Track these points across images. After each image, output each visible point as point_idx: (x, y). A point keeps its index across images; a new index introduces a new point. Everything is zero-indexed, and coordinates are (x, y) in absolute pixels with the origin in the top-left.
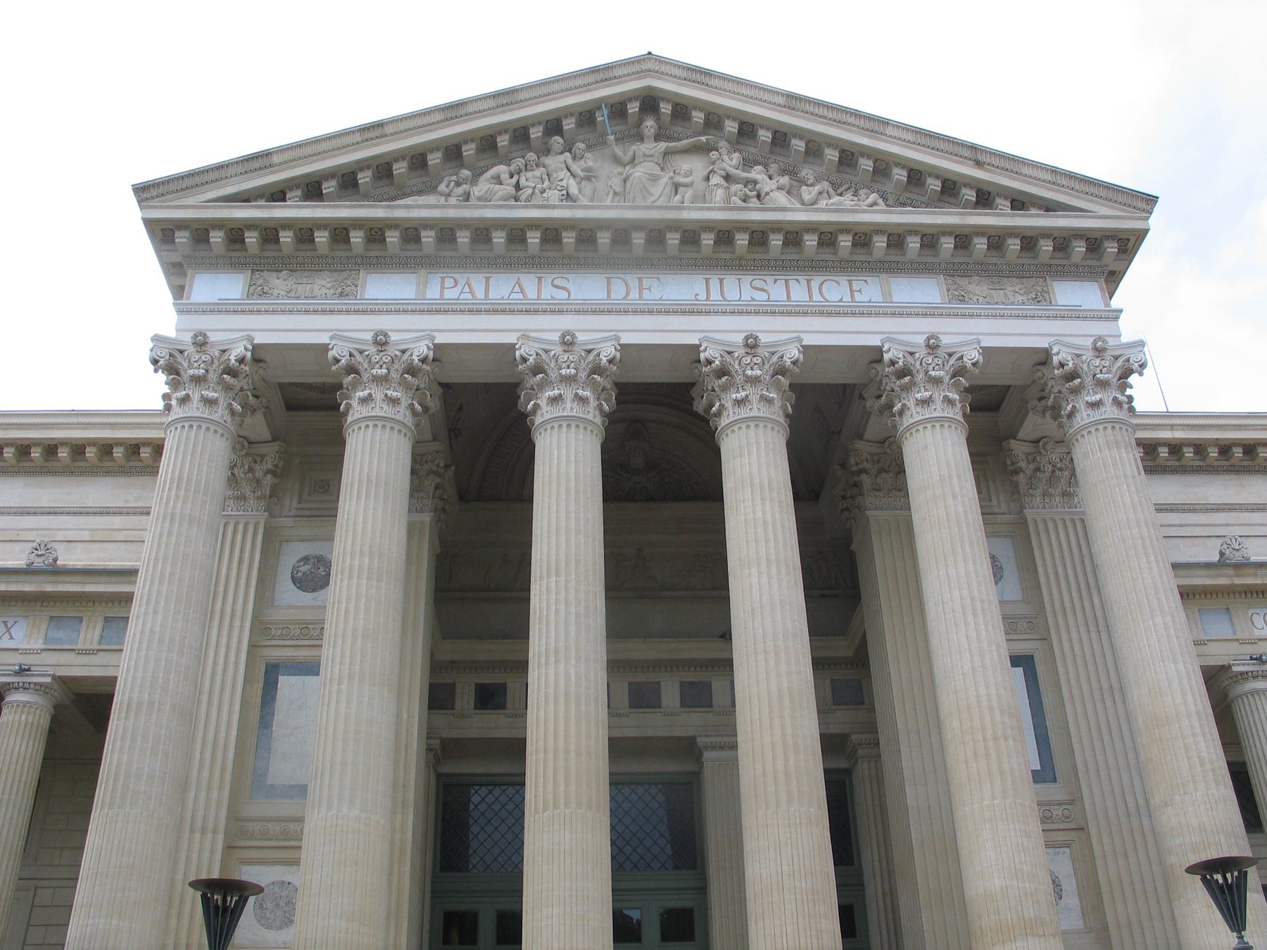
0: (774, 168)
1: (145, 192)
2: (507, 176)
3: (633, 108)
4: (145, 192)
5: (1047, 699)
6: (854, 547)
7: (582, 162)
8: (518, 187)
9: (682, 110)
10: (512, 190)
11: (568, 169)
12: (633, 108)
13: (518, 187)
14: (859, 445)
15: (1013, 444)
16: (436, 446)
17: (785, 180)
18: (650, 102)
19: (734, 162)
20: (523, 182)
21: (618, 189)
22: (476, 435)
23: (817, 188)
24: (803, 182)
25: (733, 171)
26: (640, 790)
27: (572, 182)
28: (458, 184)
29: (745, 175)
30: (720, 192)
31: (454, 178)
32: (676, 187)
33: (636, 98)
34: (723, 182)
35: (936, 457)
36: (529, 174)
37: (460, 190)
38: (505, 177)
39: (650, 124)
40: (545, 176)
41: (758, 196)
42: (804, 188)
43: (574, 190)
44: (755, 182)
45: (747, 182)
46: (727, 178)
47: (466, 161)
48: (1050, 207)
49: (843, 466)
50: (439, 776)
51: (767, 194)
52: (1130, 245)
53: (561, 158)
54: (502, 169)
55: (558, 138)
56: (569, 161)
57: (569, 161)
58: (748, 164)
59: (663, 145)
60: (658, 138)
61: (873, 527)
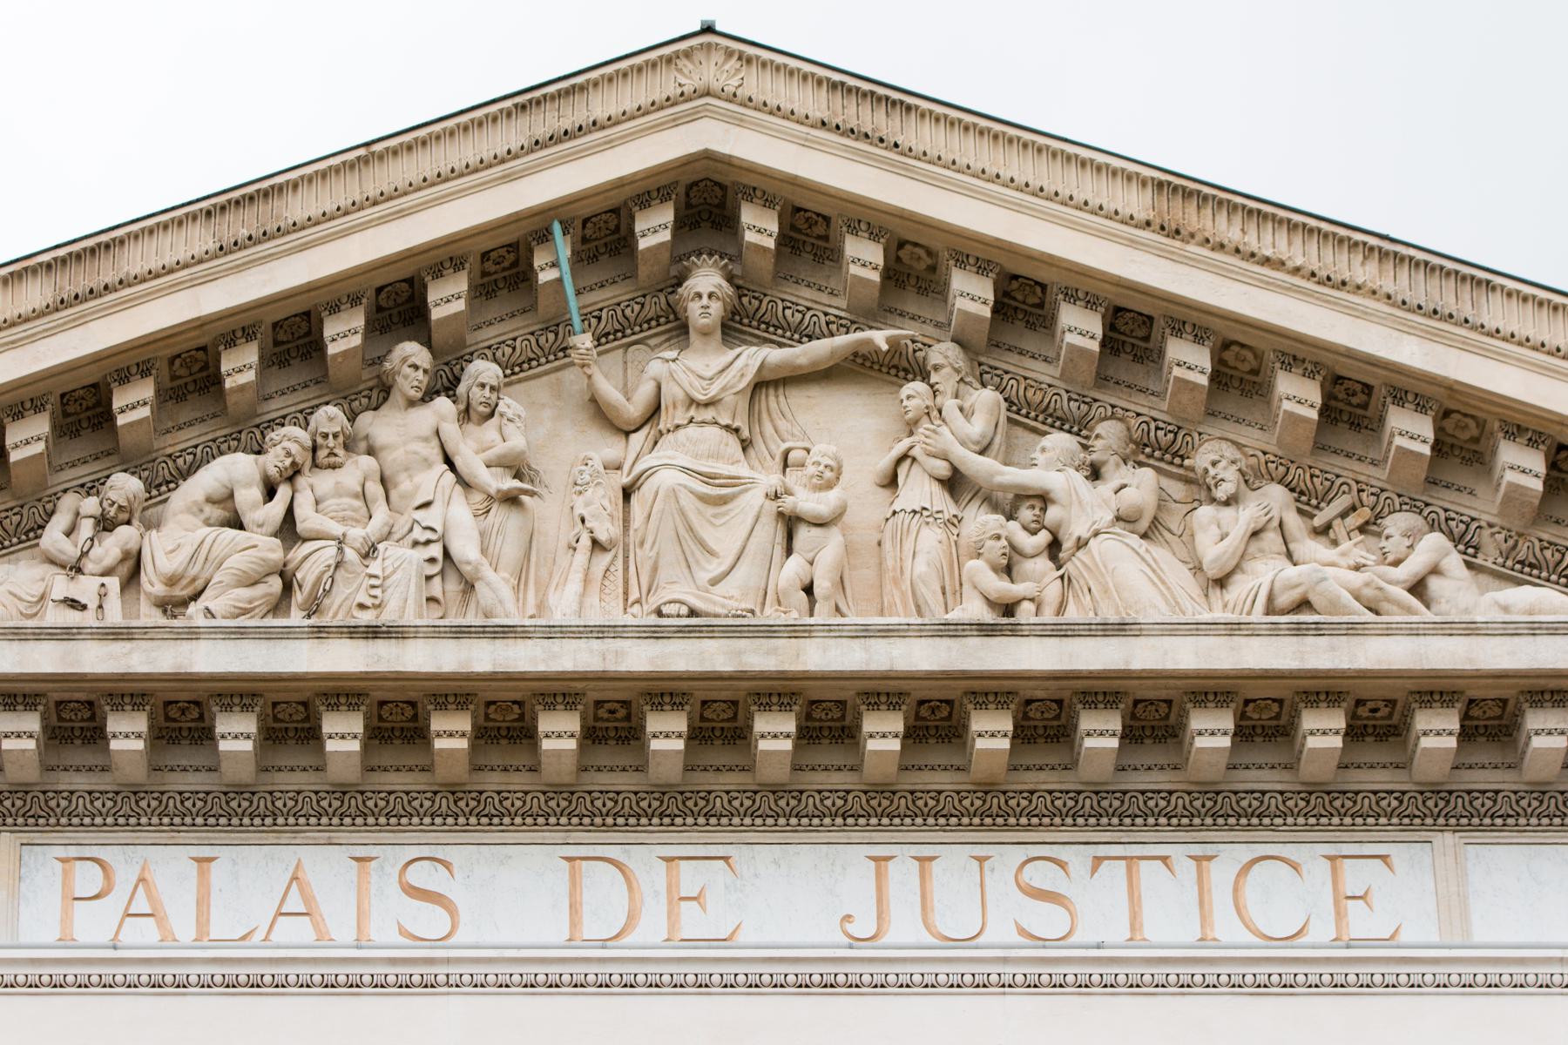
0: (1109, 434)
2: (256, 493)
7: (489, 431)
9: (812, 227)
11: (448, 461)
13: (288, 529)
19: (978, 427)
24: (1202, 488)
28: (106, 524)
31: (91, 505)
32: (790, 523)
34: (940, 500)
36: (324, 482)
37: (111, 547)
38: (249, 497)
40: (375, 489)
41: (1054, 547)
42: (1205, 512)
43: (466, 549)
44: (1044, 499)
45: (1011, 503)
46: (954, 483)
51: (1081, 544)
54: (236, 469)
56: (451, 430)
57: (451, 430)
60: (734, 328)
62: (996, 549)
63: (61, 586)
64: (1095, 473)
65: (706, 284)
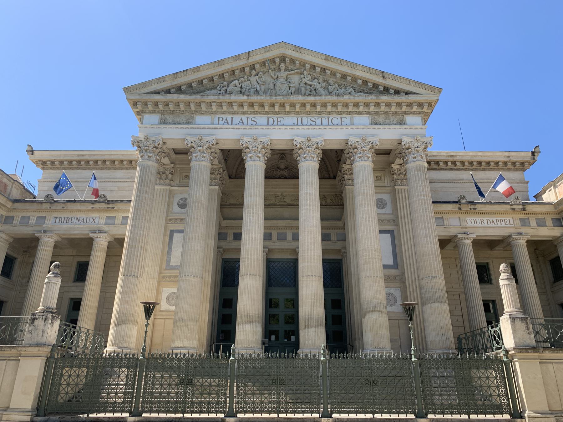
0: (321, 80)
1: (126, 90)
3: (277, 60)
4: (126, 90)
5: (397, 244)
6: (343, 195)
8: (241, 87)
9: (293, 61)
10: (240, 89)
12: (277, 60)
13: (241, 87)
14: (344, 166)
15: (393, 165)
16: (220, 166)
17: (324, 84)
18: (283, 59)
19: (308, 79)
20: (243, 86)
21: (272, 88)
22: (232, 164)
23: (334, 87)
25: (308, 82)
26: (281, 264)
27: (258, 86)
28: (223, 87)
29: (311, 83)
30: (303, 89)
33: (278, 57)
34: (305, 86)
35: (362, 174)
38: (237, 84)
39: (283, 65)
43: (258, 89)
45: (311, 86)
46: (306, 84)
47: (226, 79)
48: (407, 93)
49: (340, 171)
50: (223, 259)
52: (433, 104)
53: (255, 77)
54: (236, 82)
55: (254, 71)
58: (313, 78)
59: (287, 72)
60: (285, 70)
61: (347, 191)
62: (309, 90)
63: (219, 92)
64: (319, 83)
65: (283, 65)
